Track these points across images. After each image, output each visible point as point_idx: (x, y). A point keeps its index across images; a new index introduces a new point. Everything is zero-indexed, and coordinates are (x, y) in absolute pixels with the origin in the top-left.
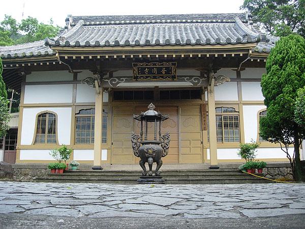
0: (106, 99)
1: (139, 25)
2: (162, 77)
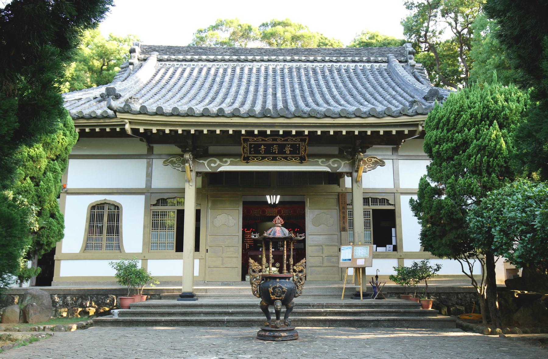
0: (200, 185)
1: (245, 64)
2: (286, 158)
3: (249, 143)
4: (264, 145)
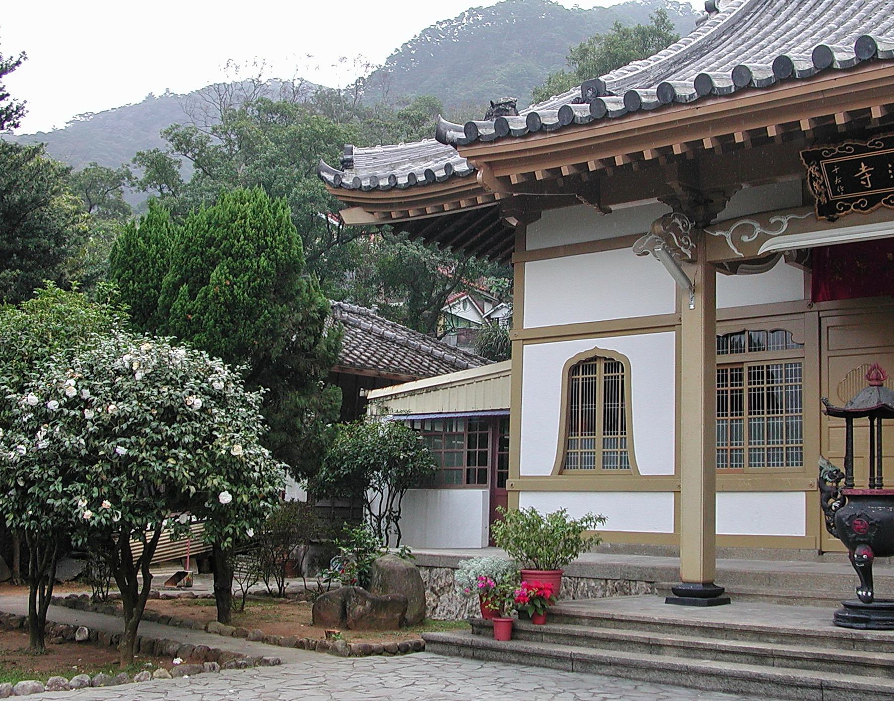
3: (823, 163)
4: (865, 160)
